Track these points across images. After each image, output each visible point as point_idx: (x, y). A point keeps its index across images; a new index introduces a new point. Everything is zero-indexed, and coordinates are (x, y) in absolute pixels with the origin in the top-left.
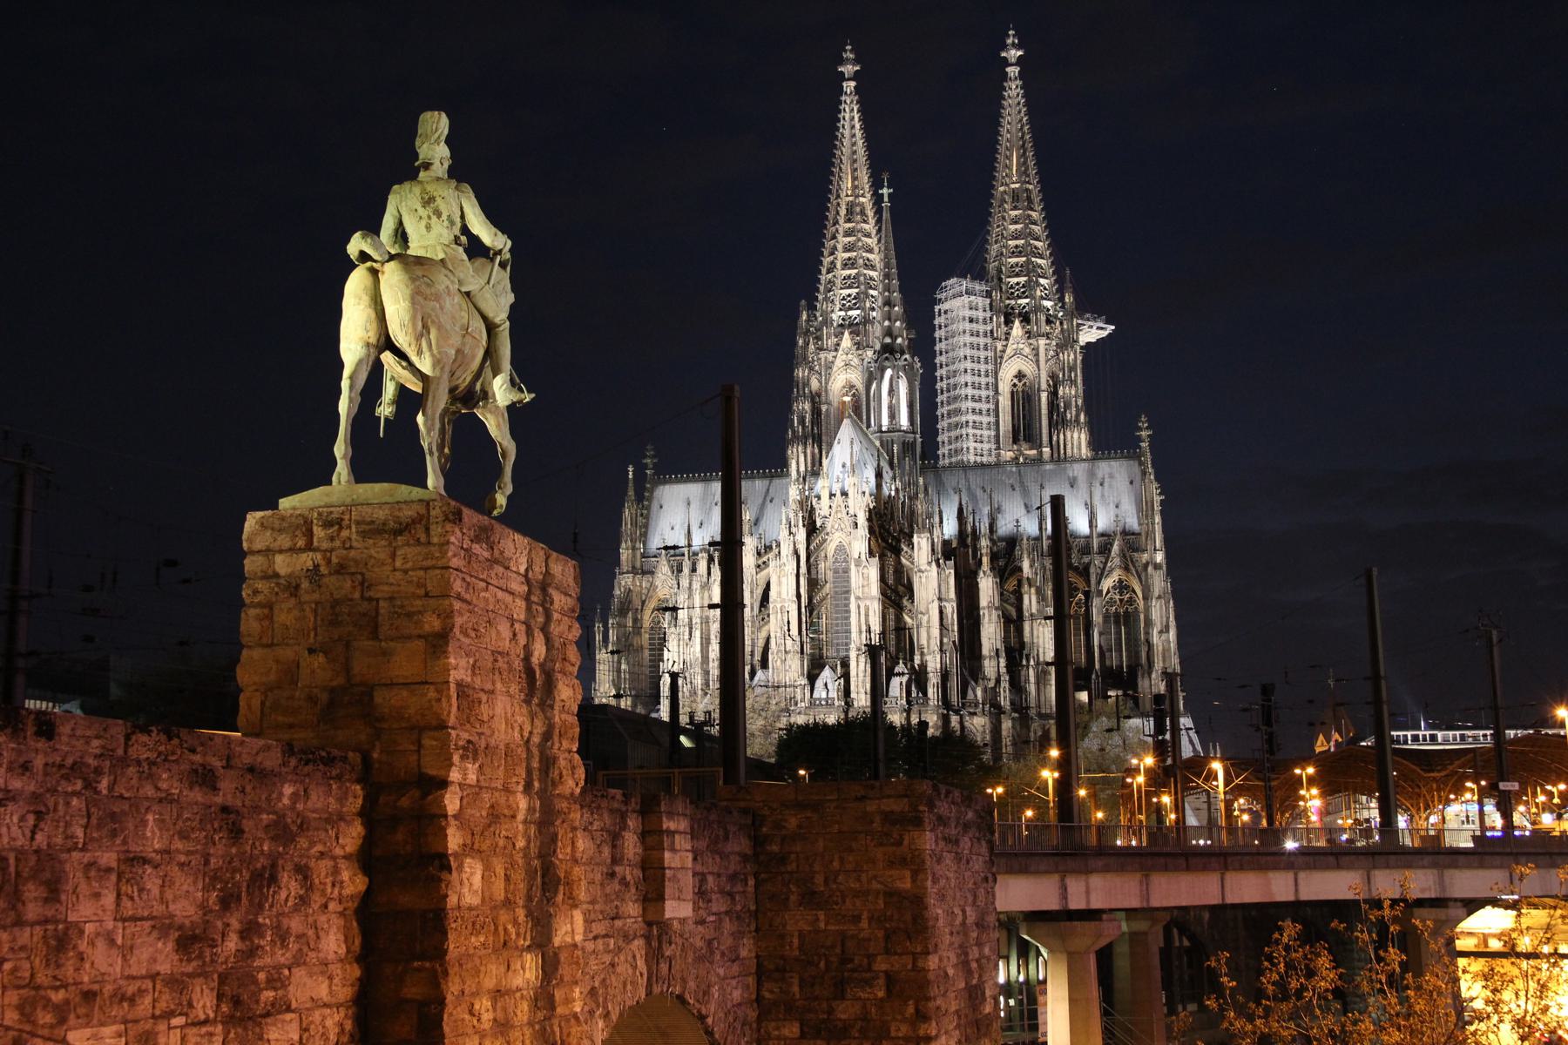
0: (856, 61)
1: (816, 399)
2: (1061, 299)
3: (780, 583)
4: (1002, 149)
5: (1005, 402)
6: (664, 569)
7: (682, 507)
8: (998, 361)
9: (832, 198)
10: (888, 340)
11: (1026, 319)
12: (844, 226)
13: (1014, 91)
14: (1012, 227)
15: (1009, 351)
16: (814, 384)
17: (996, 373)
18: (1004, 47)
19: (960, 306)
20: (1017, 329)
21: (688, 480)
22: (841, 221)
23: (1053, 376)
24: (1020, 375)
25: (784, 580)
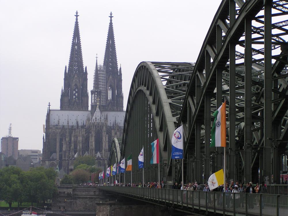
3: (91, 138)
15: (109, 81)
23: (117, 86)
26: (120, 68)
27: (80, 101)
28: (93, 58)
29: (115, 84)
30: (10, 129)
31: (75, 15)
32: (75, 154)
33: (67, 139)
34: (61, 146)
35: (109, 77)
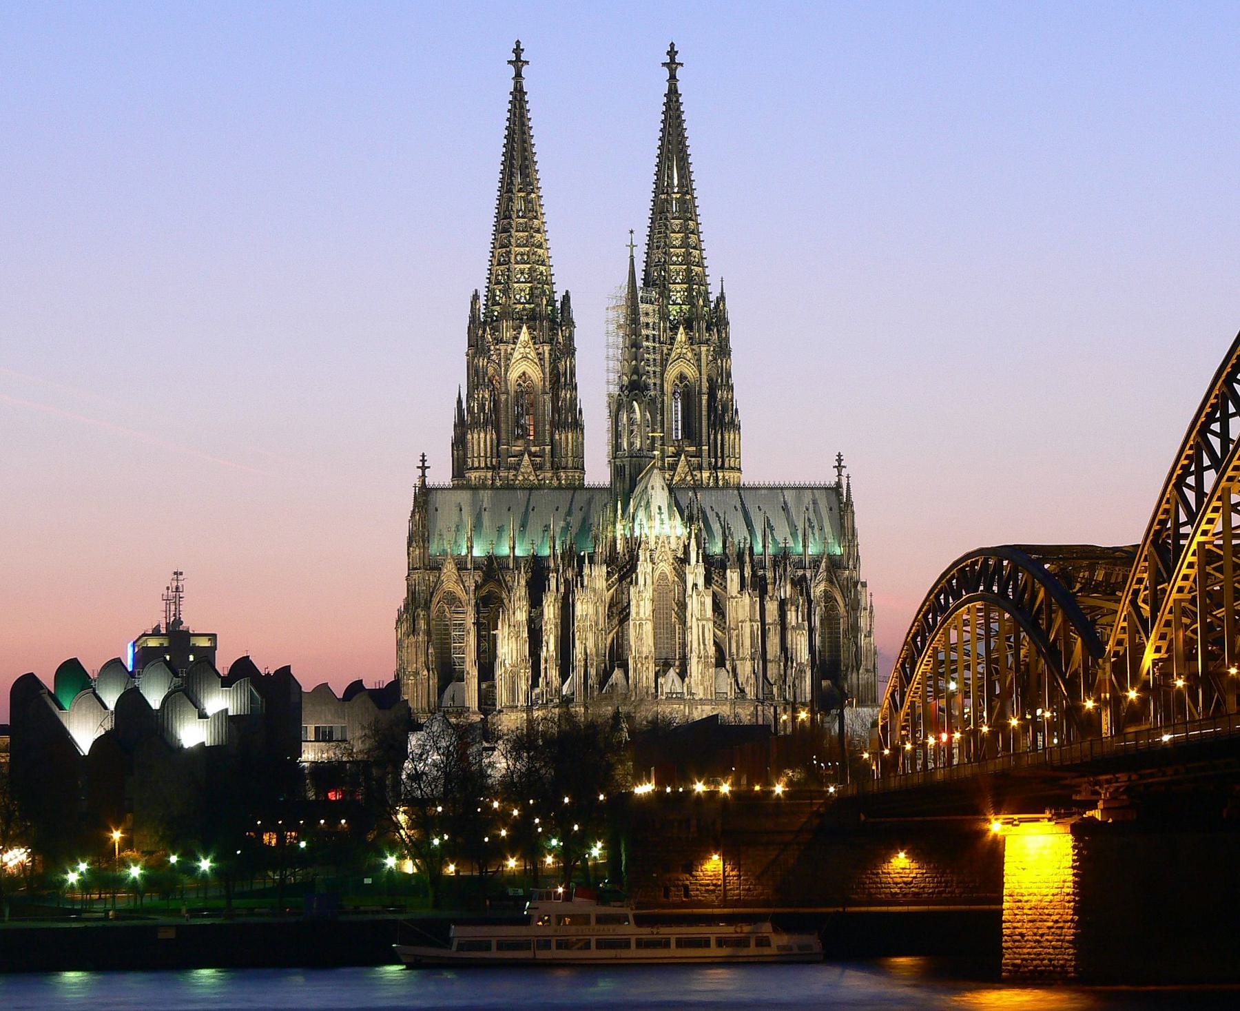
3: (638, 606)
6: (449, 570)
7: (455, 510)
8: (664, 363)
10: (635, 377)
11: (689, 327)
16: (491, 371)
17: (662, 375)
20: (681, 336)
22: (514, 216)
23: (710, 380)
25: (642, 603)
26: (722, 298)
27: (548, 448)
28: (592, 258)
29: (699, 366)
30: (175, 596)
31: (510, 62)
32: (563, 683)
33: (521, 616)
35: (673, 339)
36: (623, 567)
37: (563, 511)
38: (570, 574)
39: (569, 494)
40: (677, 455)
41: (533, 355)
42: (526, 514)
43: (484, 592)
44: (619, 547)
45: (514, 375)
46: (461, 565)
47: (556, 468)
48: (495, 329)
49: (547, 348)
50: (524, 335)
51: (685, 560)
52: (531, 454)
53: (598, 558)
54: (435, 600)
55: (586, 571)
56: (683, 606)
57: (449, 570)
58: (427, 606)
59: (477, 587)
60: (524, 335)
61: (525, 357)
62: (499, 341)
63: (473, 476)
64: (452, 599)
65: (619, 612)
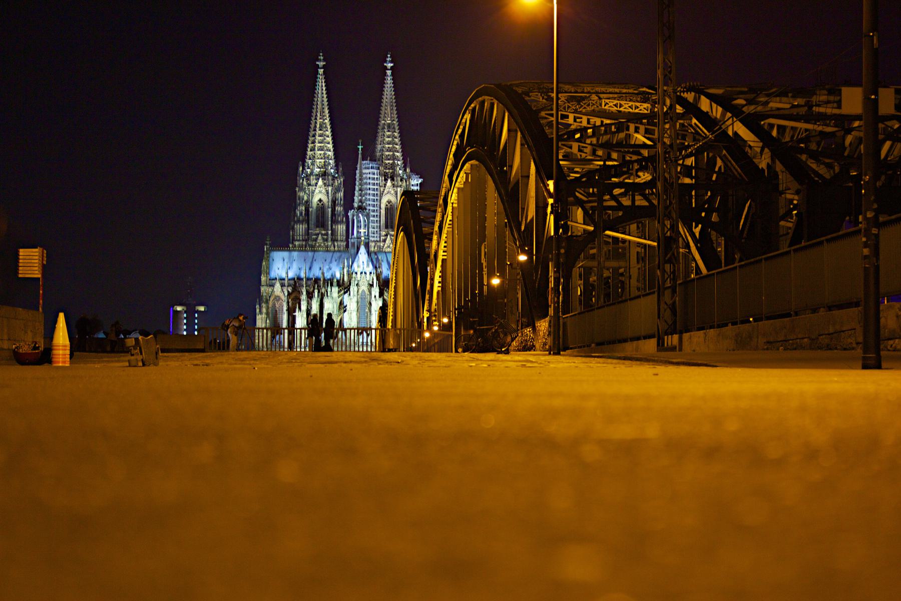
0: (324, 60)
1: (308, 204)
2: (405, 170)
4: (383, 105)
5: (383, 212)
6: (278, 286)
9: (313, 119)
11: (393, 180)
12: (318, 132)
13: (389, 80)
14: (387, 139)
16: (306, 198)
18: (386, 61)
19: (368, 172)
20: (389, 183)
21: (283, 250)
24: (389, 202)
27: (330, 232)
33: (304, 307)
34: (292, 320)
35: (385, 185)
36: (344, 287)
37: (328, 261)
38: (323, 290)
39: (331, 254)
40: (386, 235)
41: (324, 191)
42: (312, 263)
43: (293, 296)
44: (346, 279)
45: (315, 200)
46: (282, 285)
47: (333, 240)
48: (308, 180)
49: (330, 188)
50: (320, 182)
51: (372, 285)
52: (322, 235)
53: (335, 283)
54: (272, 299)
55: (329, 289)
56: (370, 304)
57: (278, 286)
58: (267, 302)
59: (289, 294)
60: (320, 182)
61: (320, 192)
62: (309, 185)
63: (297, 243)
64: (278, 298)
65: (342, 307)
